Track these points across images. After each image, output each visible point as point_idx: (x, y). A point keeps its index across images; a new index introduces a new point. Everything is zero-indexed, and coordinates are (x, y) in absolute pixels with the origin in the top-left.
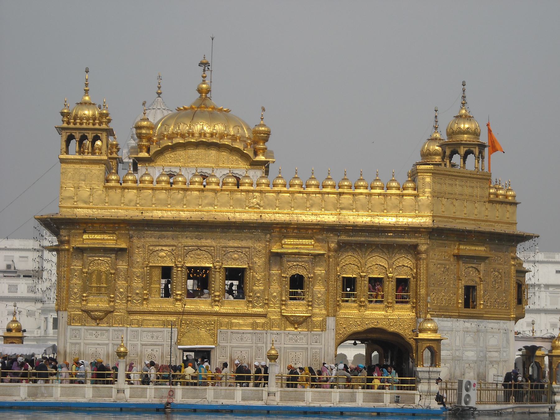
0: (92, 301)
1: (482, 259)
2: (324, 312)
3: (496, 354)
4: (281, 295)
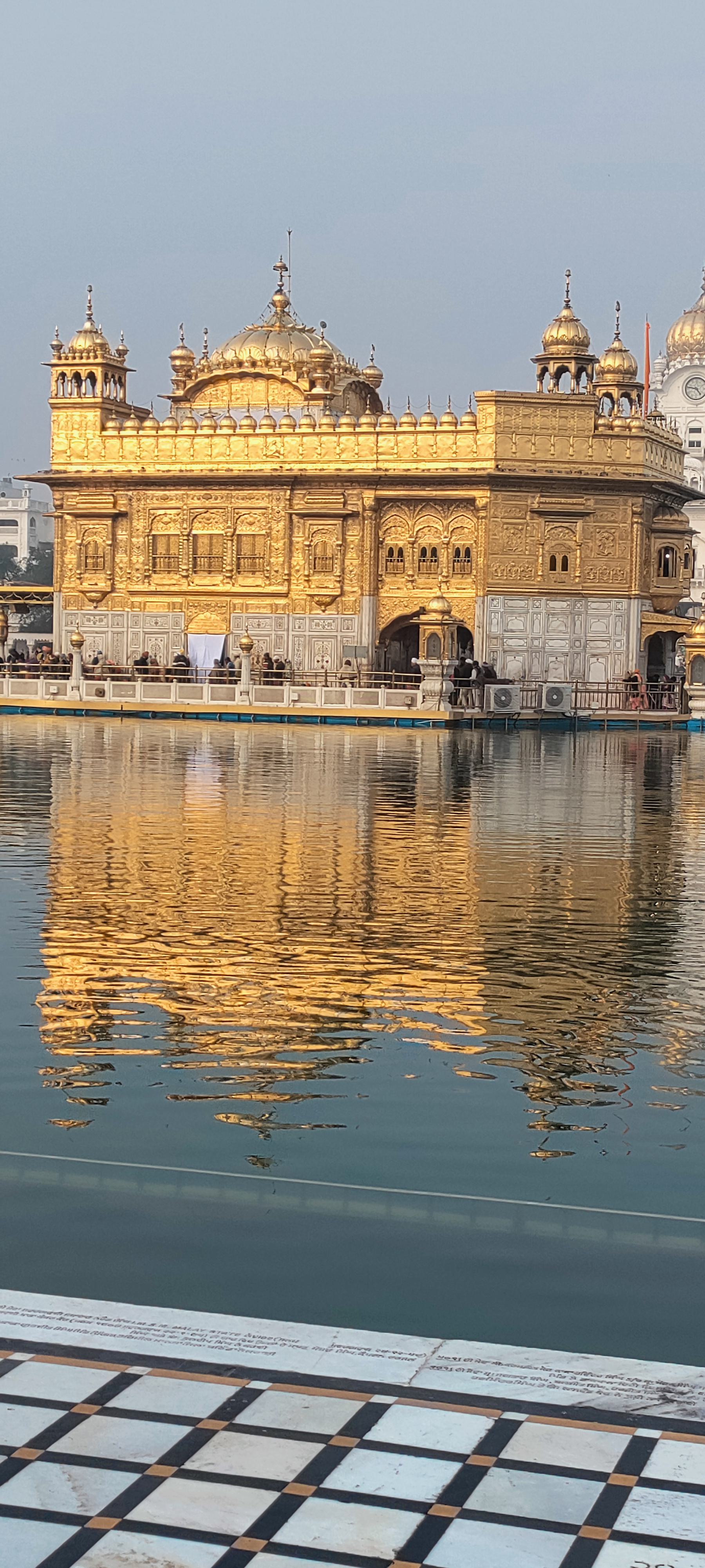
0: (87, 579)
3: (605, 644)
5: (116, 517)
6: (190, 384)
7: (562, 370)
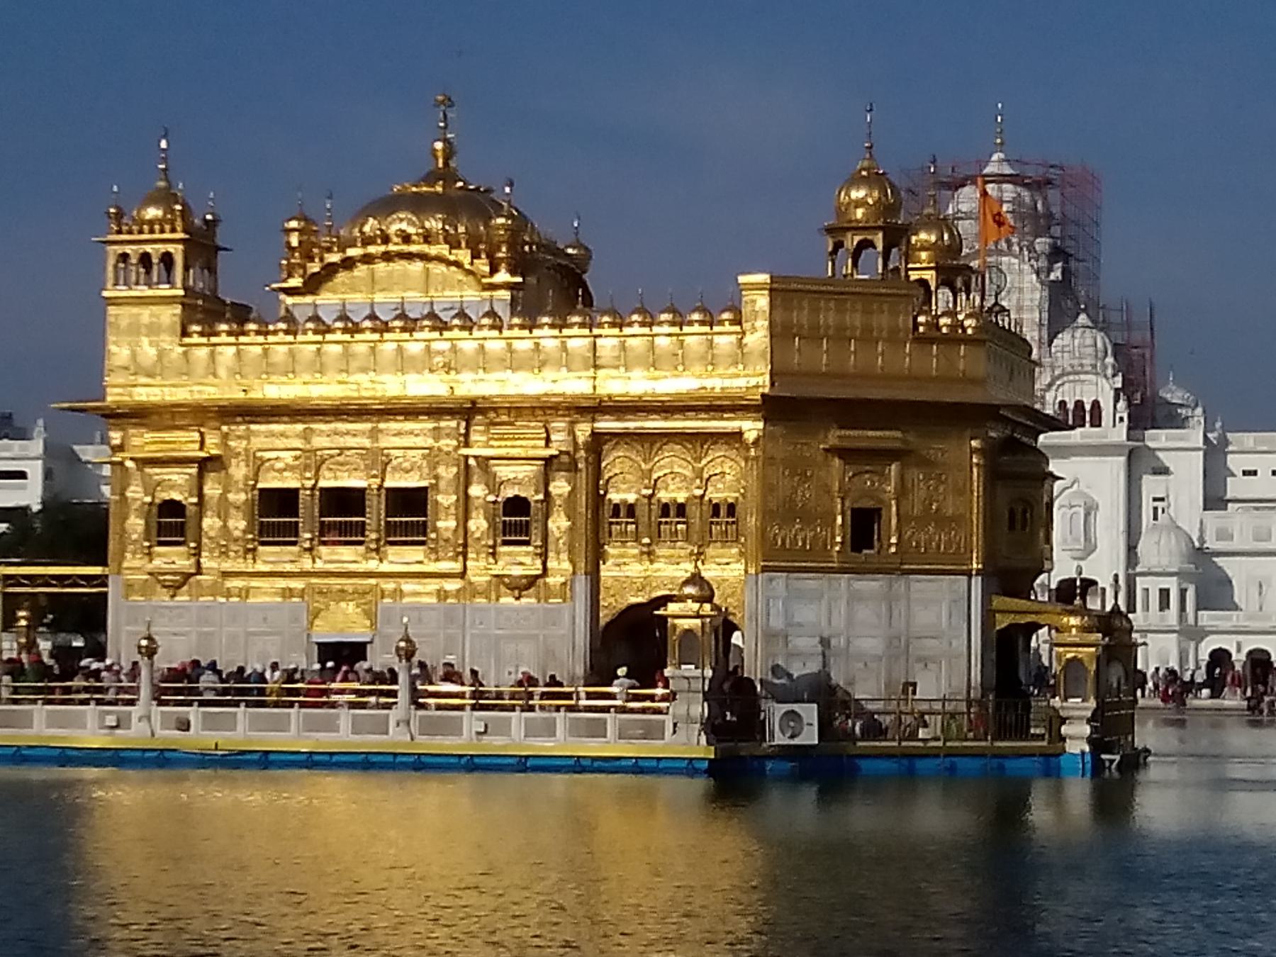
0: (159, 555)
2: (567, 565)
7: (866, 244)
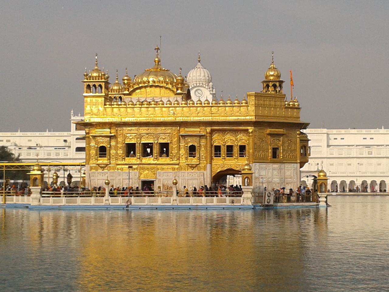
0: (100, 160)
1: (283, 135)
3: (290, 179)
4: (185, 155)
5: (110, 137)
6: (131, 89)
